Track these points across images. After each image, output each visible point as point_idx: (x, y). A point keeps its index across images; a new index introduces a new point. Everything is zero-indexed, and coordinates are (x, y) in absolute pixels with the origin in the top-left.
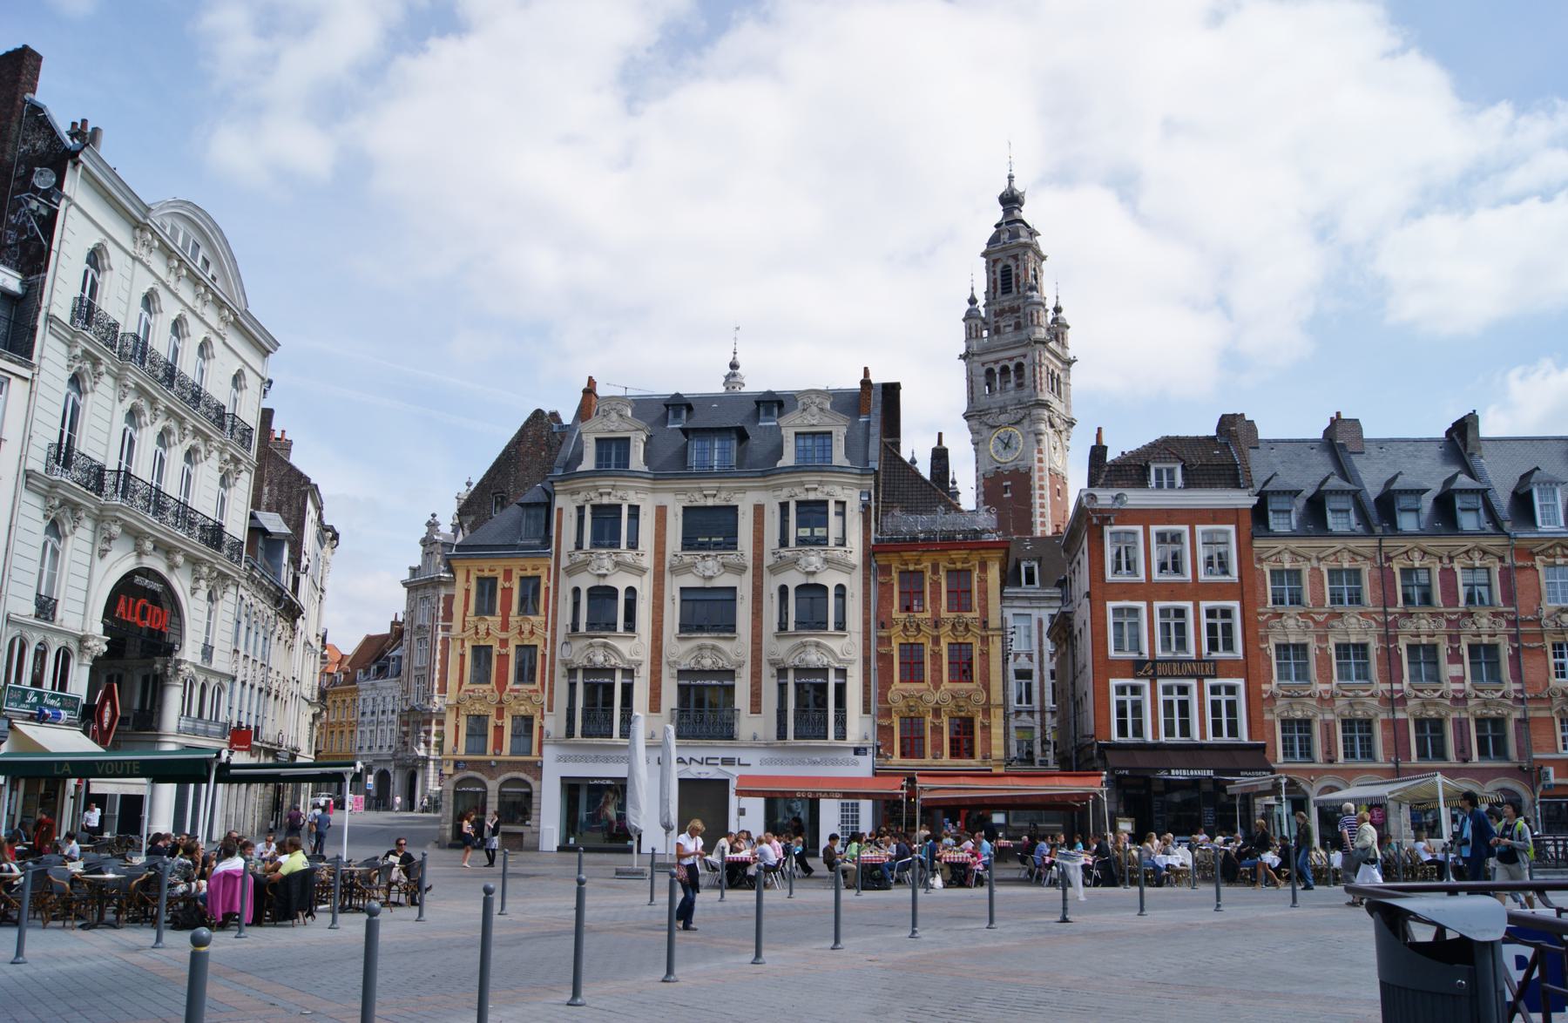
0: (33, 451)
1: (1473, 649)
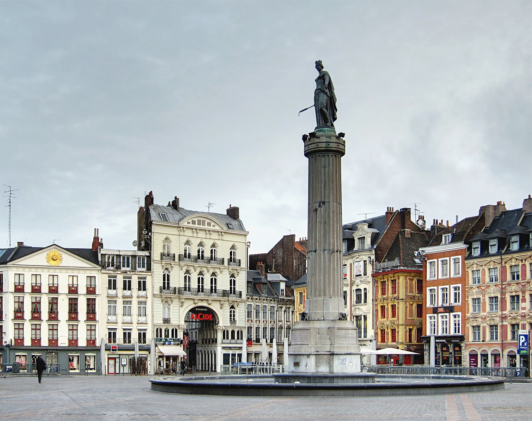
0: (155, 289)
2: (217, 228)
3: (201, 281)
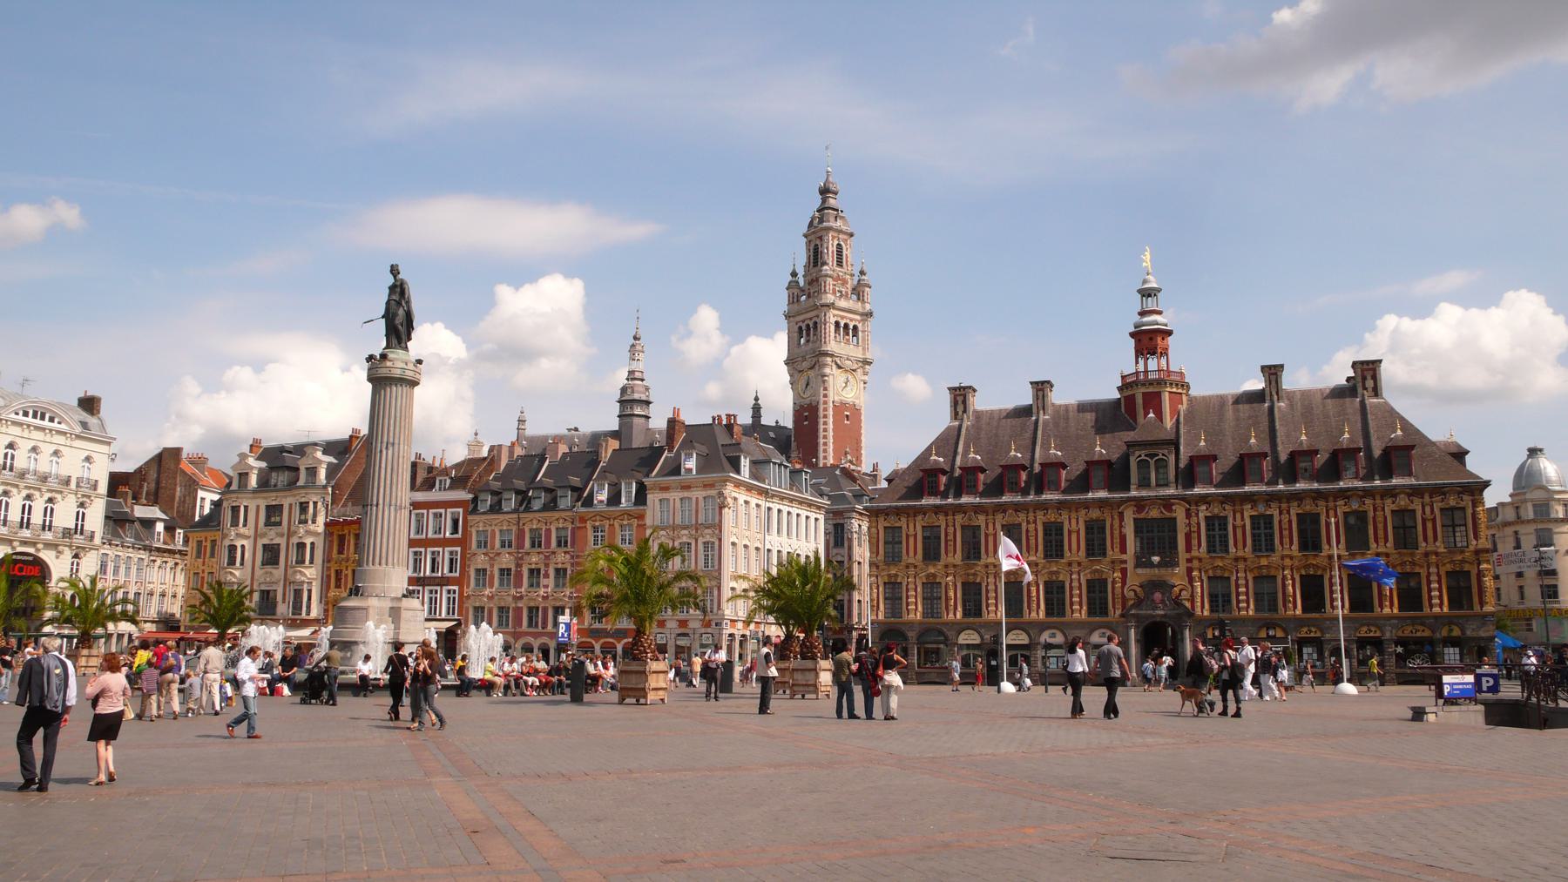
1: (557, 570)
2: (63, 427)
3: (26, 510)
